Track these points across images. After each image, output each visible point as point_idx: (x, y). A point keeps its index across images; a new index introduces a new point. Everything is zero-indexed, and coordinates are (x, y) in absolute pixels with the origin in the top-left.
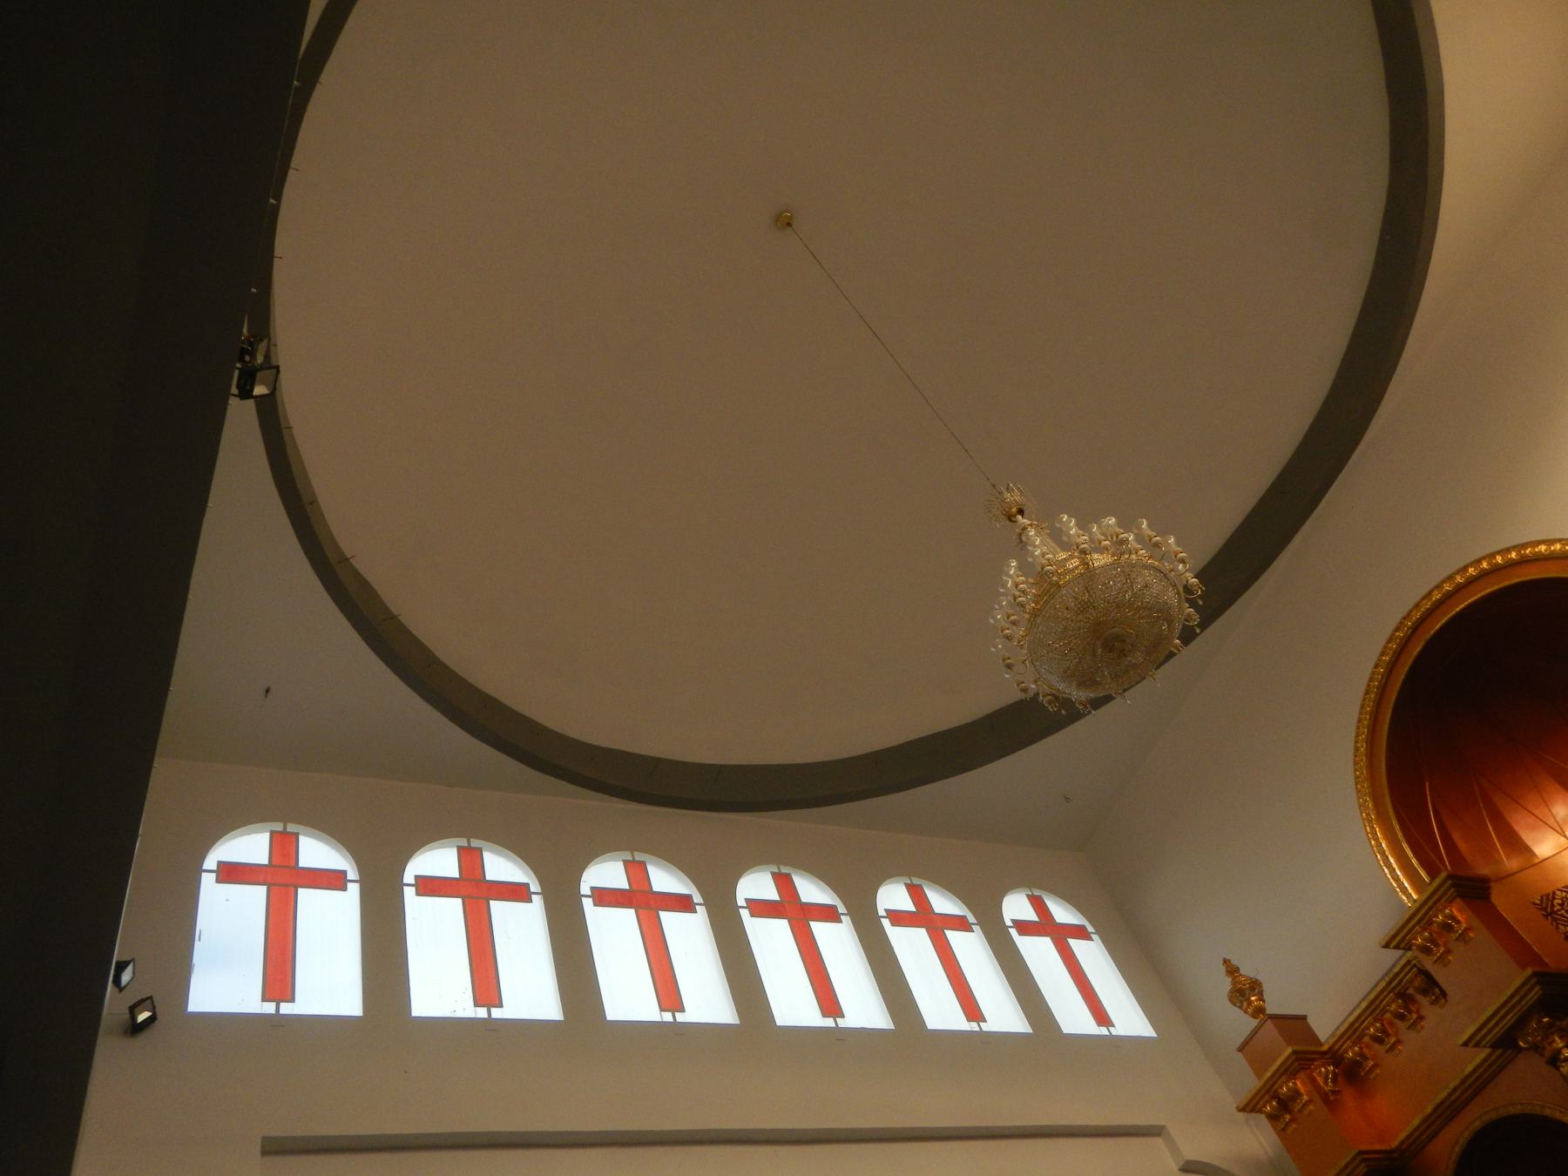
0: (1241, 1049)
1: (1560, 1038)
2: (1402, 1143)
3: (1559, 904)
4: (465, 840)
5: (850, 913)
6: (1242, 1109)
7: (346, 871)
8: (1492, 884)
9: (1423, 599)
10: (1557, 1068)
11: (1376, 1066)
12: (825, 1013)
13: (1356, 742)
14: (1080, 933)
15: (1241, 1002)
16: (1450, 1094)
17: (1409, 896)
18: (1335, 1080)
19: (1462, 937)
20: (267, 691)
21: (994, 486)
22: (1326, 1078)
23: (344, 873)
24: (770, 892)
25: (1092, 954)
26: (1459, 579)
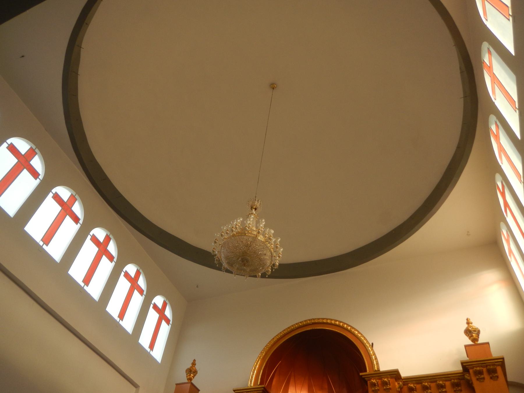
0: (177, 384)
5: (116, 263)
9: (321, 319)
13: (275, 337)
14: (168, 321)
15: (188, 373)
20: (23, 56)
21: (256, 197)
25: (165, 329)
26: (333, 322)
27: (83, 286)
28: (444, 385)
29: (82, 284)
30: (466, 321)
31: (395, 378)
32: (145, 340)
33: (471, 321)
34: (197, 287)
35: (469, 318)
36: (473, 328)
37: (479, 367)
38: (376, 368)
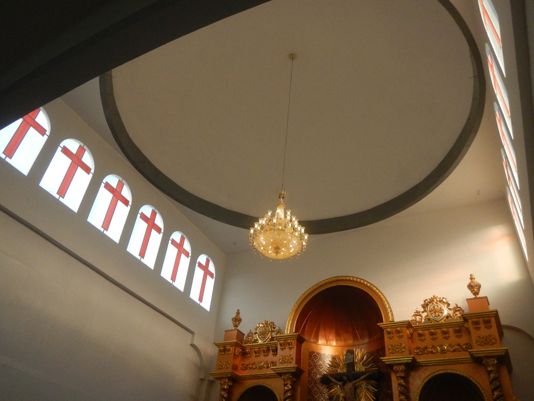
0: (225, 331)
1: (290, 382)
2: (242, 376)
3: (314, 355)
4: (83, 144)
6: (215, 344)
7: (47, 131)
8: (305, 341)
9: (345, 276)
10: (285, 387)
11: (250, 357)
12: (140, 255)
13: (305, 292)
14: (211, 275)
16: (260, 374)
17: (287, 331)
18: (239, 353)
19: (290, 348)
22: (238, 352)
23: (46, 131)
24: (148, 214)
25: (210, 282)
27: (140, 259)
28: (447, 331)
29: (139, 258)
30: (470, 277)
31: (406, 327)
32: (194, 295)
33: (474, 277)
34: (235, 244)
35: (473, 274)
36: (475, 284)
37: (476, 318)
38: (391, 320)
